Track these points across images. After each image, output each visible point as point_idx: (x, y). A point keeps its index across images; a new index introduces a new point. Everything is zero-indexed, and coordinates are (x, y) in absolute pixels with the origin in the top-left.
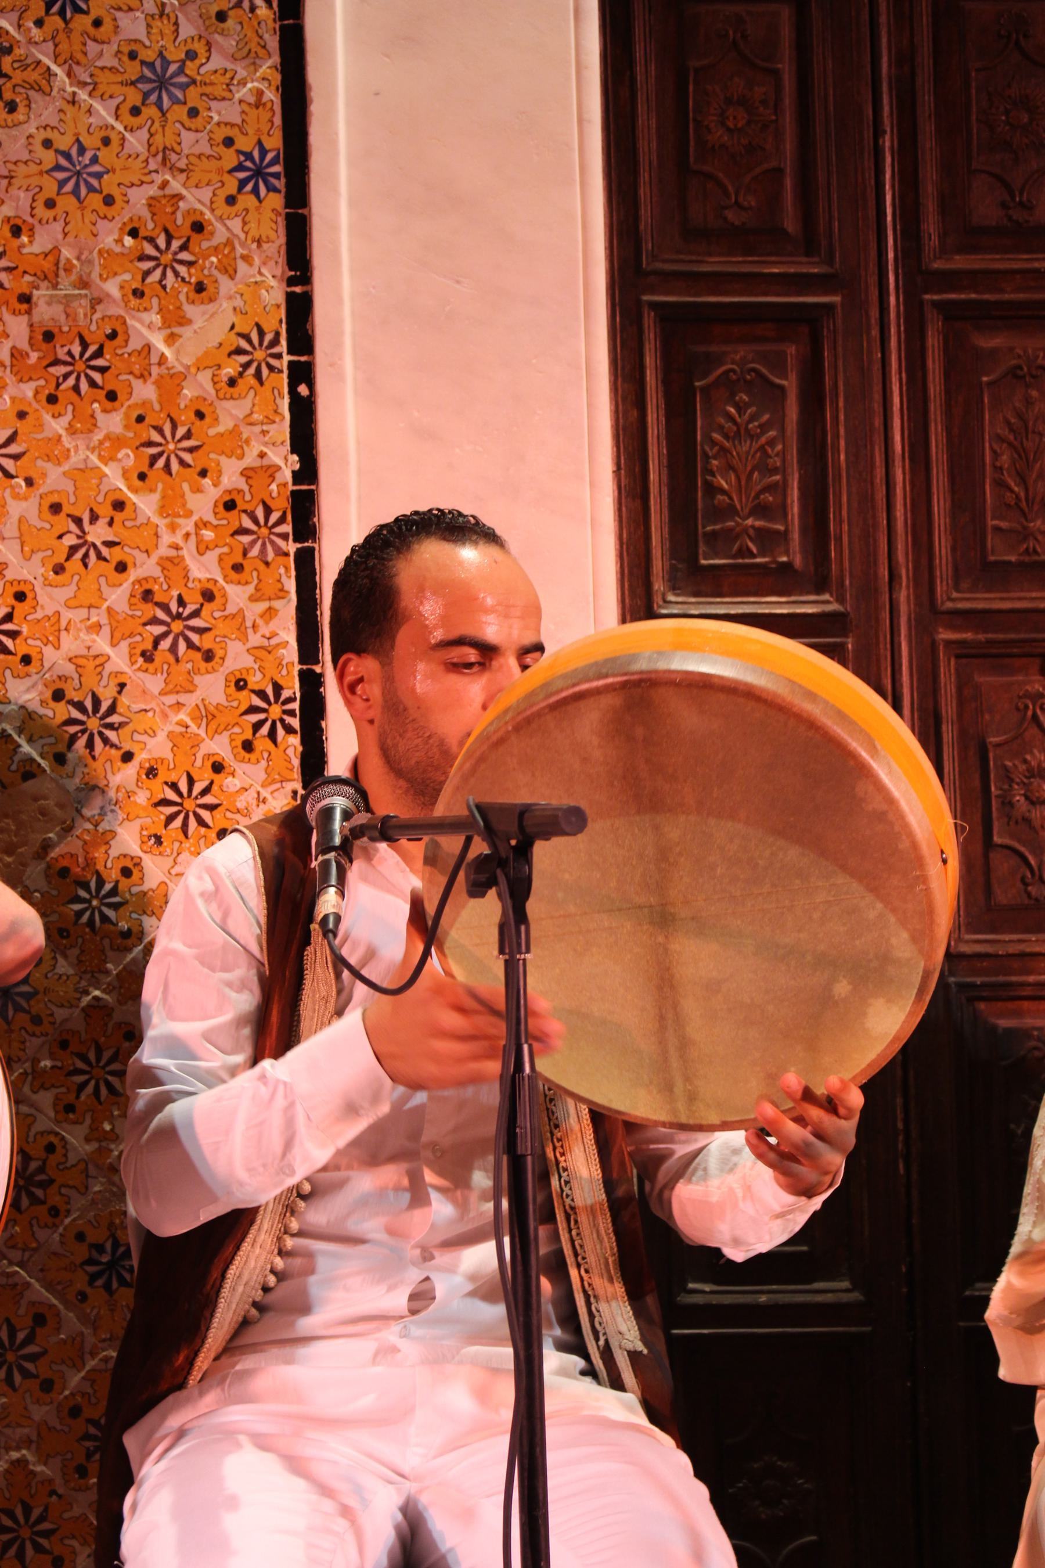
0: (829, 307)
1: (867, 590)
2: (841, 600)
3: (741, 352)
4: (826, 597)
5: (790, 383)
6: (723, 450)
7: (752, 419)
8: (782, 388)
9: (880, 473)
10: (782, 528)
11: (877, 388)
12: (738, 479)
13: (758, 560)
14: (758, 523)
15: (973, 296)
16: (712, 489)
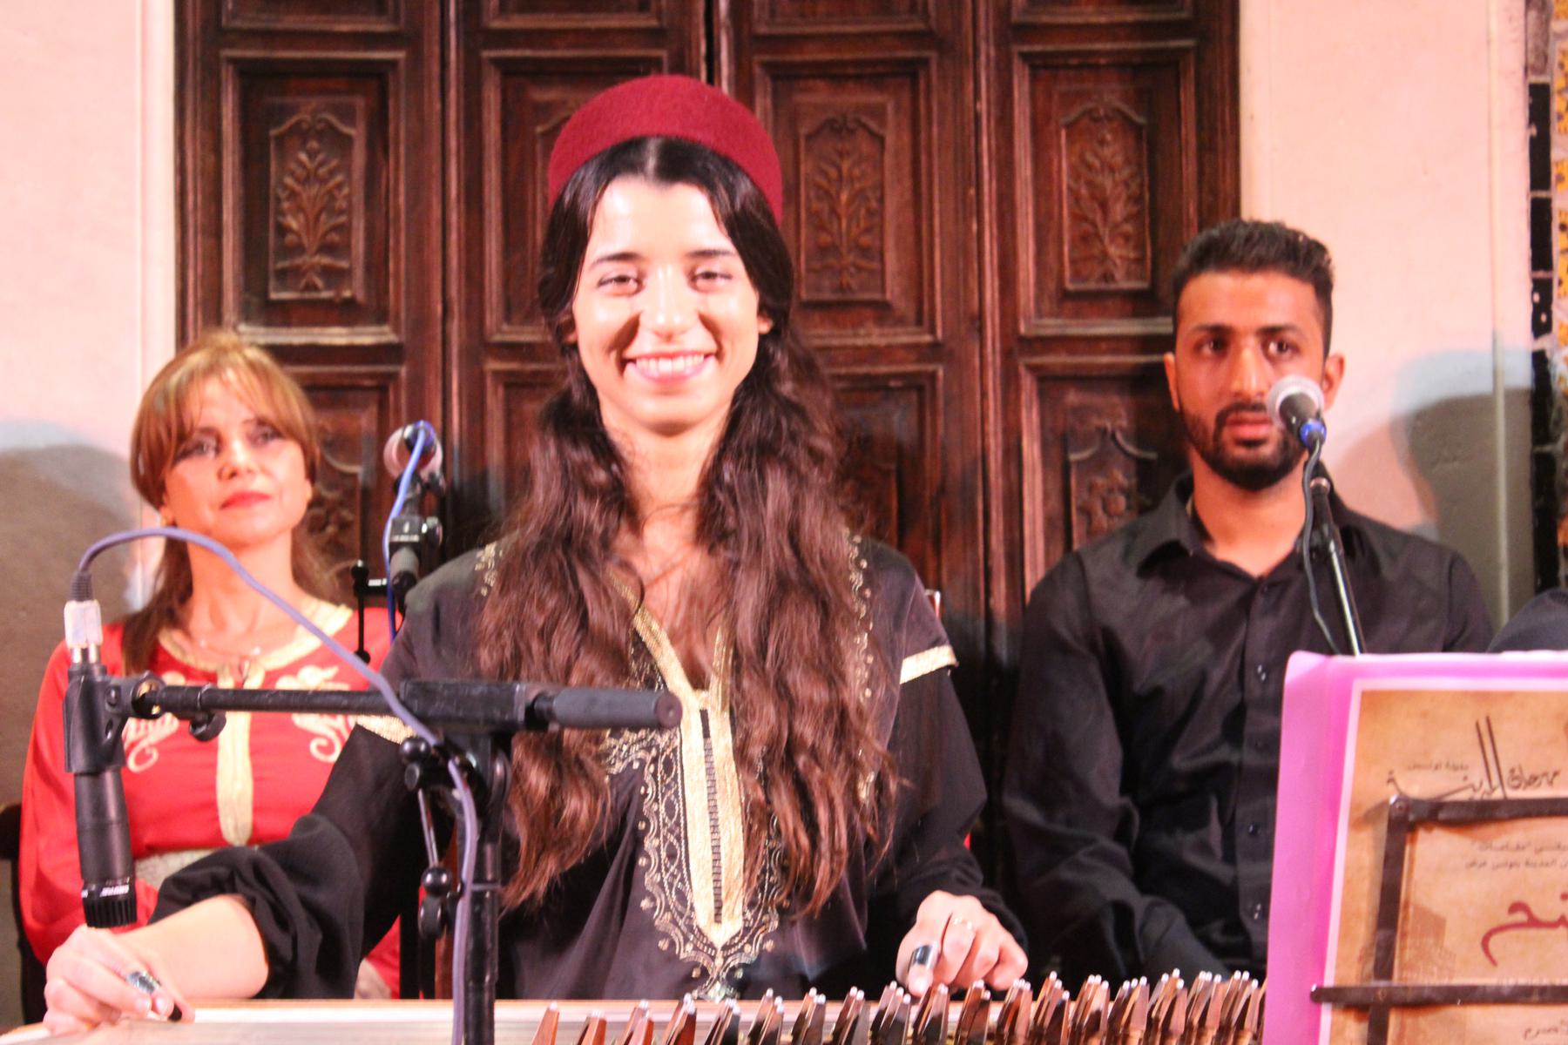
0: (393, 64)
1: (420, 323)
2: (396, 330)
3: (314, 102)
4: (386, 328)
5: (357, 132)
6: (293, 195)
7: (321, 165)
8: (349, 139)
9: (436, 212)
10: (344, 264)
11: (436, 136)
12: (307, 219)
13: (326, 295)
14: (326, 260)
15: (528, 53)
16: (282, 230)
